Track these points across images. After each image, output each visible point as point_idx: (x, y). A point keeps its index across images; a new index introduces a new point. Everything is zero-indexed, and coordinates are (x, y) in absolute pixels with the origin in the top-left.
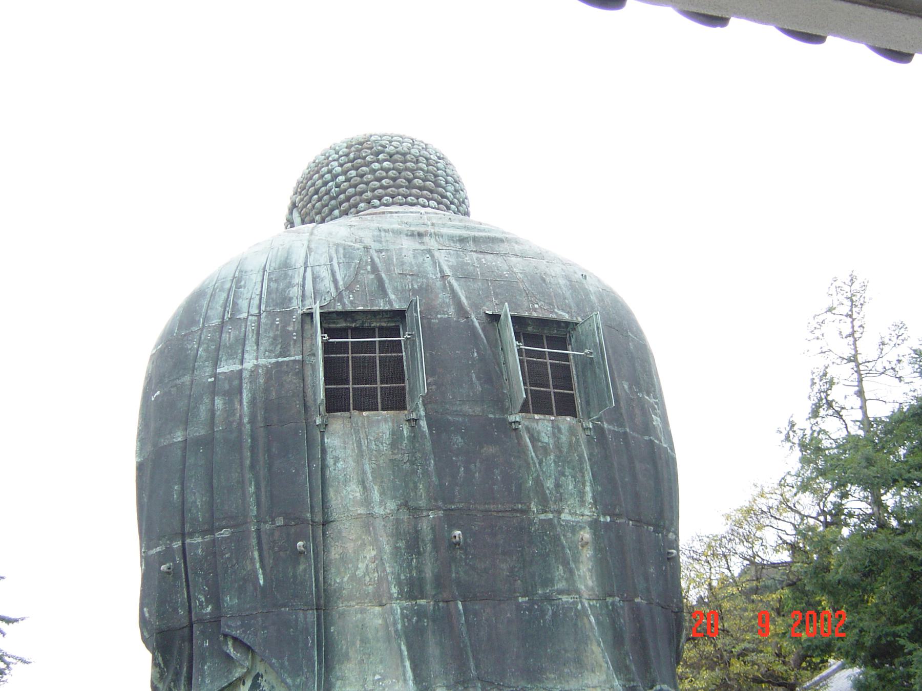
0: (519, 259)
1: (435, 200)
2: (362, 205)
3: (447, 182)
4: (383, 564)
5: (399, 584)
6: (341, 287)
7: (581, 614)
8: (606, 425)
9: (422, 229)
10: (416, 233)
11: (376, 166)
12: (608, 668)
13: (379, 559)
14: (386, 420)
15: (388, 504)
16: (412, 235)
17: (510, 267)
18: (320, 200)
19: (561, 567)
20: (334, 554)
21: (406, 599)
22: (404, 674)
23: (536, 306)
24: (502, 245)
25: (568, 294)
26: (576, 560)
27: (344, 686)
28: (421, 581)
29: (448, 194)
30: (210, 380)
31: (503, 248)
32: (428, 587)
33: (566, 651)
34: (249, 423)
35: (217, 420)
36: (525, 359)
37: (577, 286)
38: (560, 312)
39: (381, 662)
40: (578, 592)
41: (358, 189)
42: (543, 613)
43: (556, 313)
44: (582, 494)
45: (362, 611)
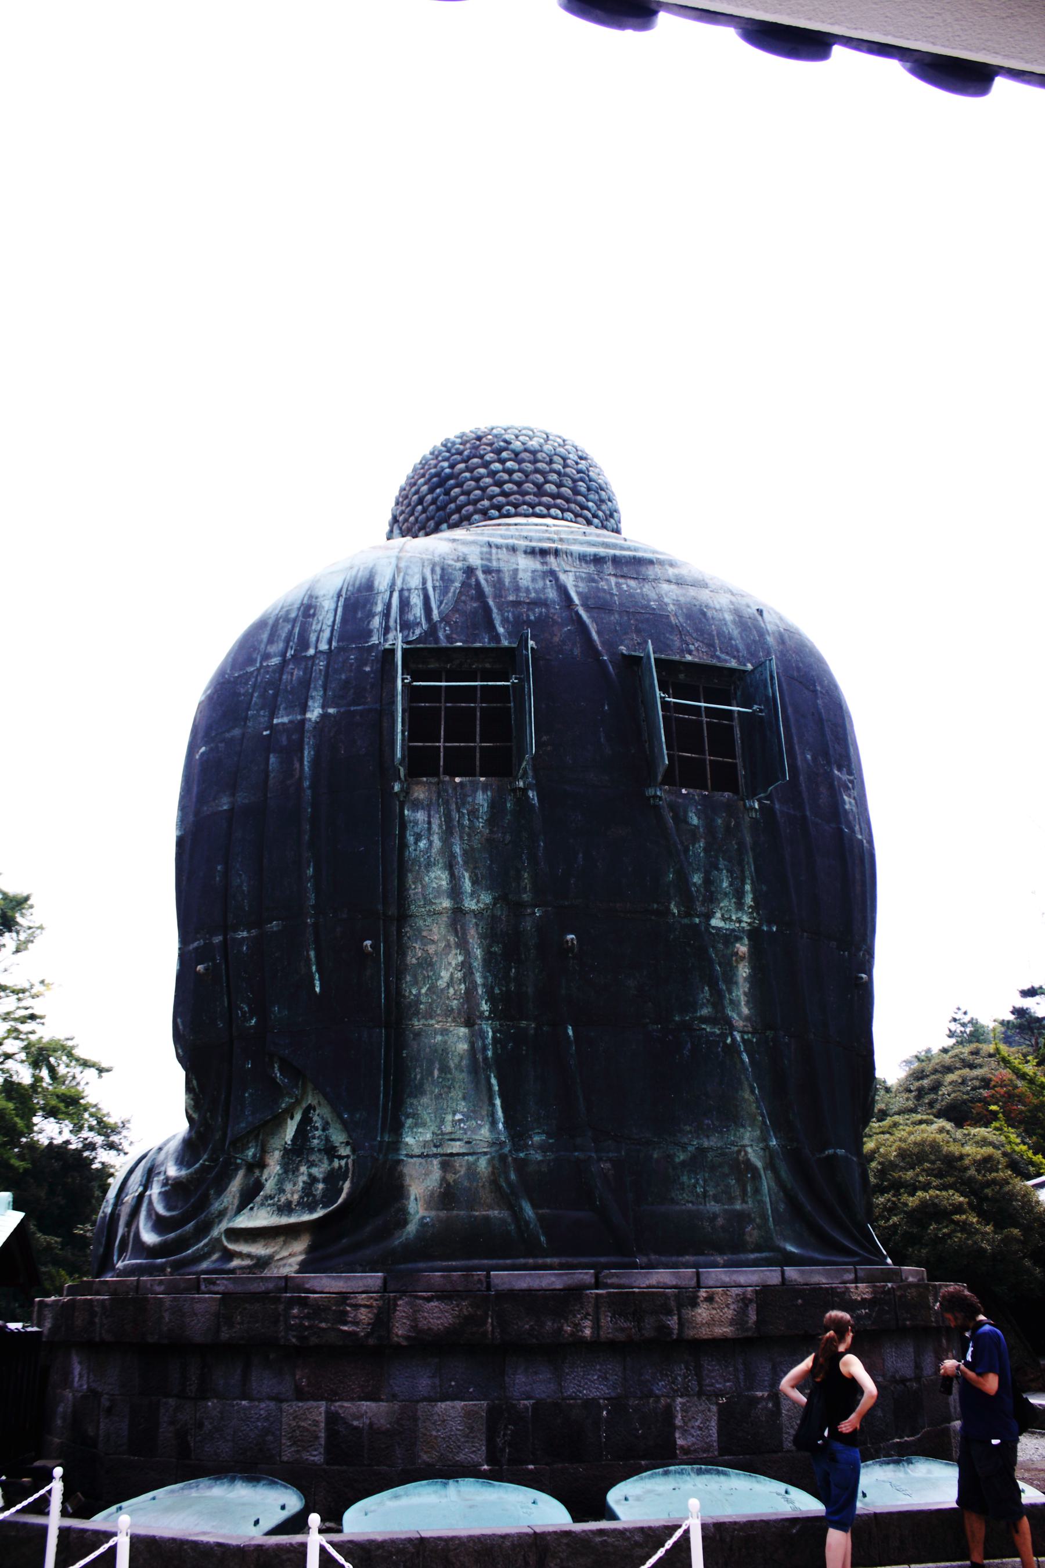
0: (673, 587)
1: (572, 512)
2: (476, 517)
3: (589, 489)
4: (472, 973)
5: (492, 999)
6: (435, 615)
7: (732, 1050)
8: (777, 806)
9: (546, 545)
10: (537, 550)
11: (497, 466)
12: (764, 1123)
13: (466, 967)
14: (485, 788)
15: (482, 897)
16: (532, 552)
17: (660, 598)
18: (424, 511)
19: (707, 988)
21: (499, 1019)
22: (492, 1115)
23: (692, 647)
24: (651, 568)
25: (736, 633)
26: (730, 980)
27: (416, 1125)
29: (590, 504)
30: (265, 733)
31: (651, 572)
34: (310, 787)
35: (271, 782)
37: (751, 624)
38: (723, 656)
39: (464, 1098)
40: (728, 1022)
41: (472, 497)
43: (718, 658)
44: (739, 895)
45: (444, 1032)
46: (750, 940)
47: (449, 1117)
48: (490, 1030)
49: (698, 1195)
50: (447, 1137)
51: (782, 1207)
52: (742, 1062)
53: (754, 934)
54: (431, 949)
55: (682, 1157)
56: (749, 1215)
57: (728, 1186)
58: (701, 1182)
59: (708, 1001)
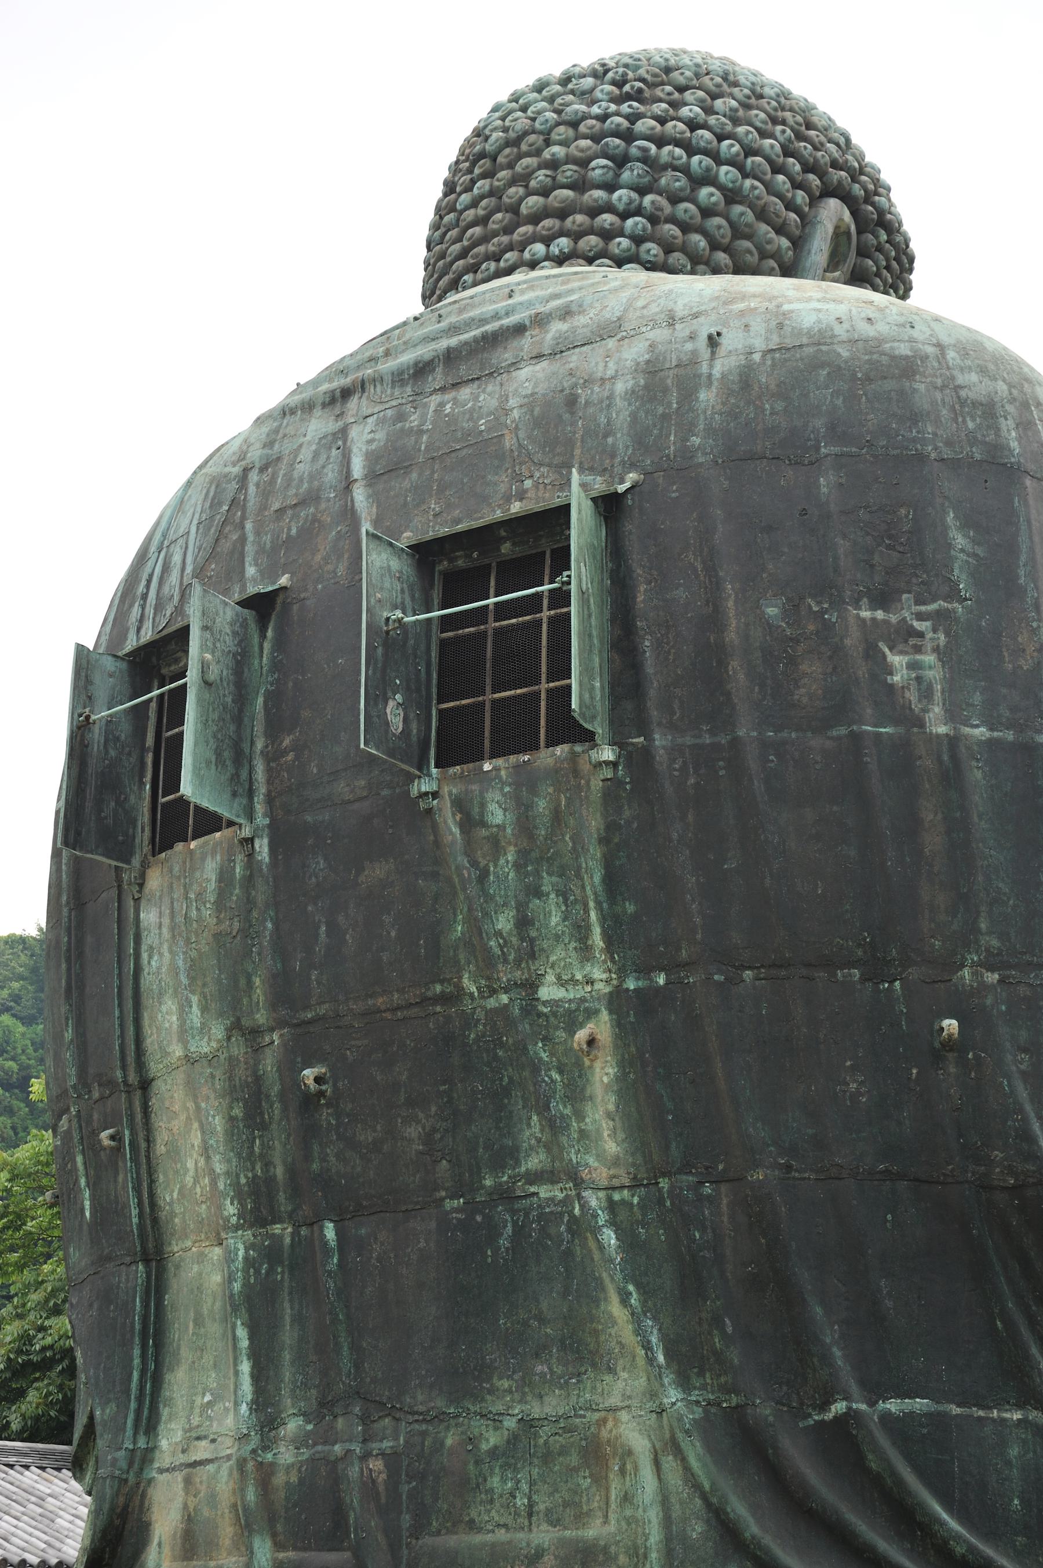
5: (239, 1196)
12: (651, 1360)
15: (213, 1031)
19: (535, 1118)
20: (160, 1149)
21: (251, 1226)
26: (577, 1094)
28: (270, 1181)
32: (282, 1197)
33: (542, 1320)
36: (546, 614)
42: (493, 1231)
44: (581, 931)
46: (611, 1012)
47: (198, 1401)
48: (241, 1247)
49: (517, 1514)
50: (194, 1435)
51: (697, 1530)
52: (601, 1248)
53: (617, 1000)
54: (176, 1125)
55: (492, 1441)
56: (605, 1549)
57: (576, 1491)
58: (525, 1486)
59: (539, 1141)
